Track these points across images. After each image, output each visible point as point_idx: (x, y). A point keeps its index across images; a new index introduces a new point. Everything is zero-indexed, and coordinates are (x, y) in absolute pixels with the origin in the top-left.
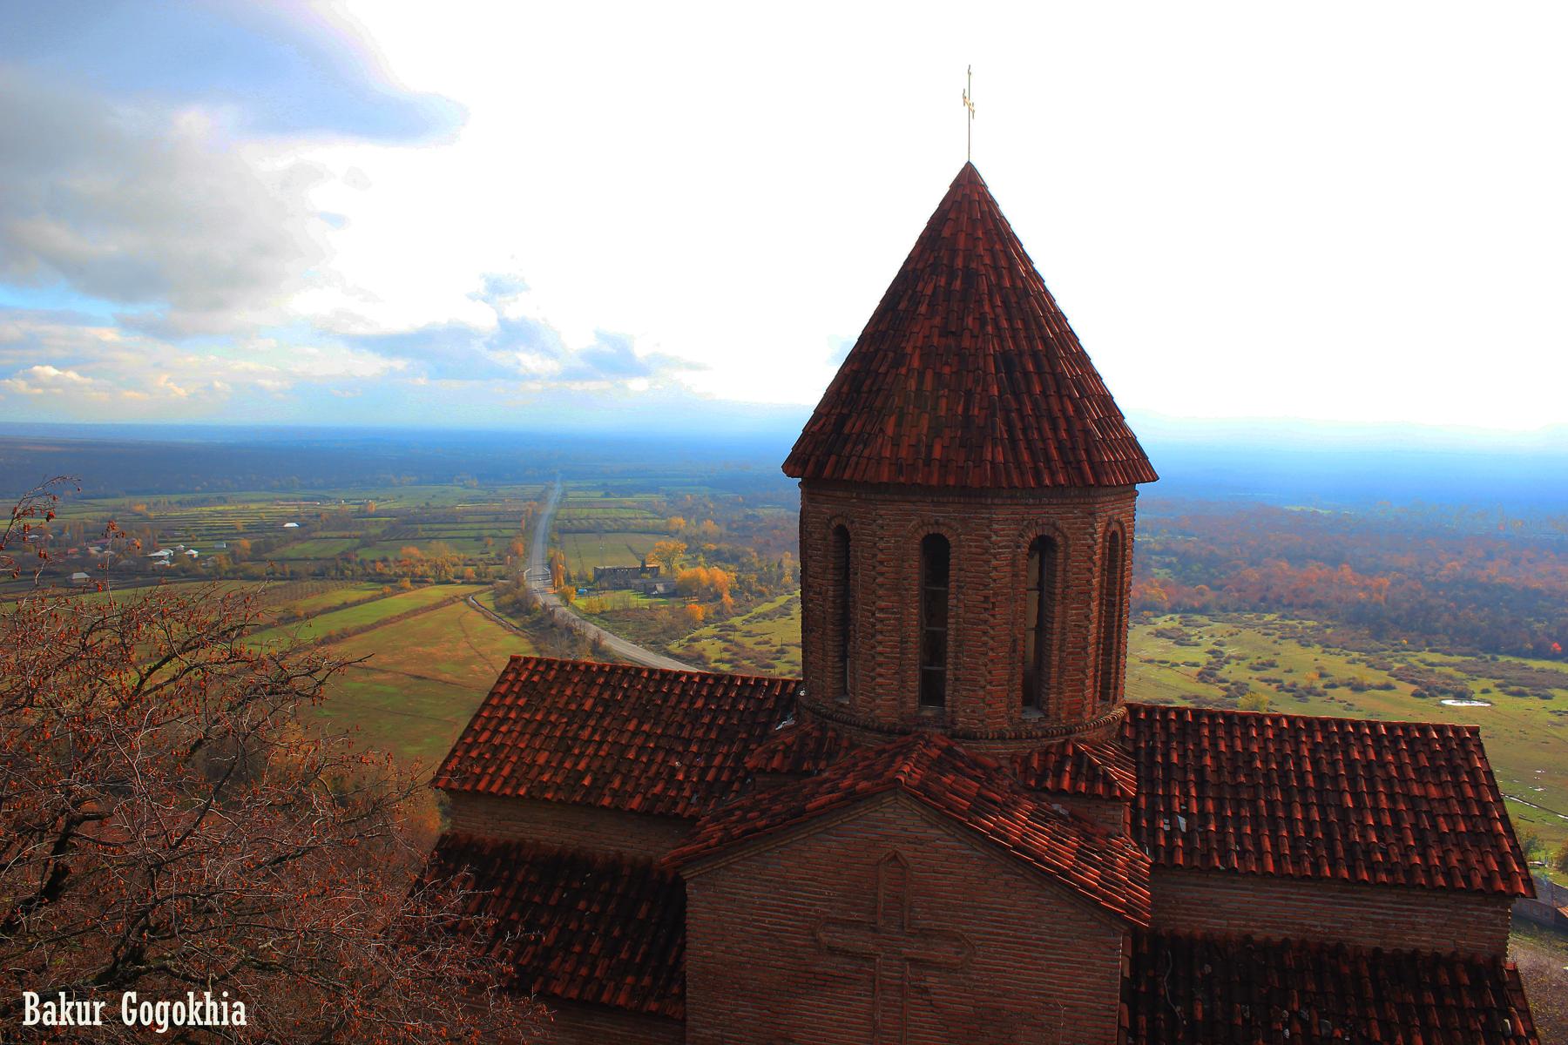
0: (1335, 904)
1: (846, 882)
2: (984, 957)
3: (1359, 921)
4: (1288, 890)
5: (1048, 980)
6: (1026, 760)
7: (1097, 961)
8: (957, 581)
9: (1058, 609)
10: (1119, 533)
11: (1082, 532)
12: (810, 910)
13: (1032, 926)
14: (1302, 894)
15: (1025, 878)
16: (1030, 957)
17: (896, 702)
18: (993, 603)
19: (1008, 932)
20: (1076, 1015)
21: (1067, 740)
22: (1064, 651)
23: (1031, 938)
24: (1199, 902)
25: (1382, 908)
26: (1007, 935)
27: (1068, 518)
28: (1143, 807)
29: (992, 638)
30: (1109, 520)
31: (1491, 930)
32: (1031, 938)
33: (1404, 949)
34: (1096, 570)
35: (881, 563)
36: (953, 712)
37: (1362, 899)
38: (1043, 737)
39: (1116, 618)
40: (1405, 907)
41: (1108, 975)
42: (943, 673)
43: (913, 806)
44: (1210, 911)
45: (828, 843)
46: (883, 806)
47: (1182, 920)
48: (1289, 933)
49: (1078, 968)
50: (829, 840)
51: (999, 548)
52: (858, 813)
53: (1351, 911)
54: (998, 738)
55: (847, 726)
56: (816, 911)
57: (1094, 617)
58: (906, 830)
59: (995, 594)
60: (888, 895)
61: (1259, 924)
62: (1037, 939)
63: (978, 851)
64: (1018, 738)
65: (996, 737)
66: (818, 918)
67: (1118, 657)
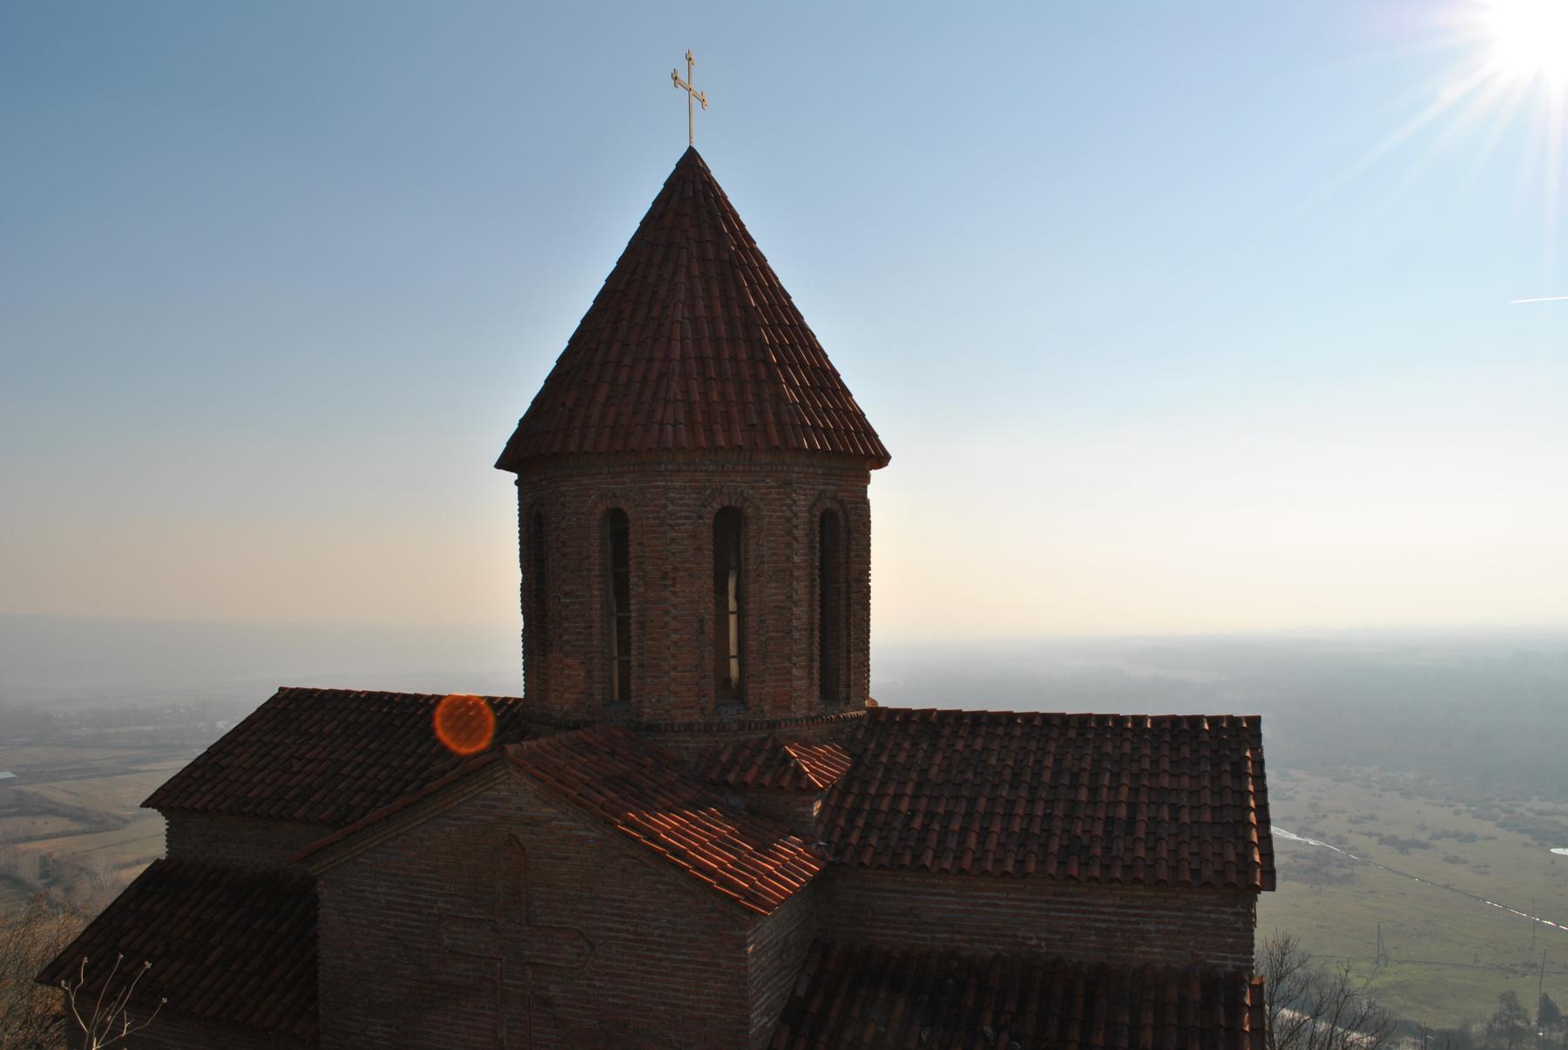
4: (996, 894)
10: (840, 513)
12: (432, 908)
13: (653, 920)
14: (1014, 899)
18: (674, 579)
19: (629, 927)
25: (1104, 913)
26: (628, 932)
30: (820, 495)
37: (1085, 904)
40: (1131, 911)
42: (630, 662)
46: (498, 781)
48: (1000, 947)
51: (680, 518)
56: (439, 908)
61: (966, 937)
62: (660, 936)
63: (592, 831)
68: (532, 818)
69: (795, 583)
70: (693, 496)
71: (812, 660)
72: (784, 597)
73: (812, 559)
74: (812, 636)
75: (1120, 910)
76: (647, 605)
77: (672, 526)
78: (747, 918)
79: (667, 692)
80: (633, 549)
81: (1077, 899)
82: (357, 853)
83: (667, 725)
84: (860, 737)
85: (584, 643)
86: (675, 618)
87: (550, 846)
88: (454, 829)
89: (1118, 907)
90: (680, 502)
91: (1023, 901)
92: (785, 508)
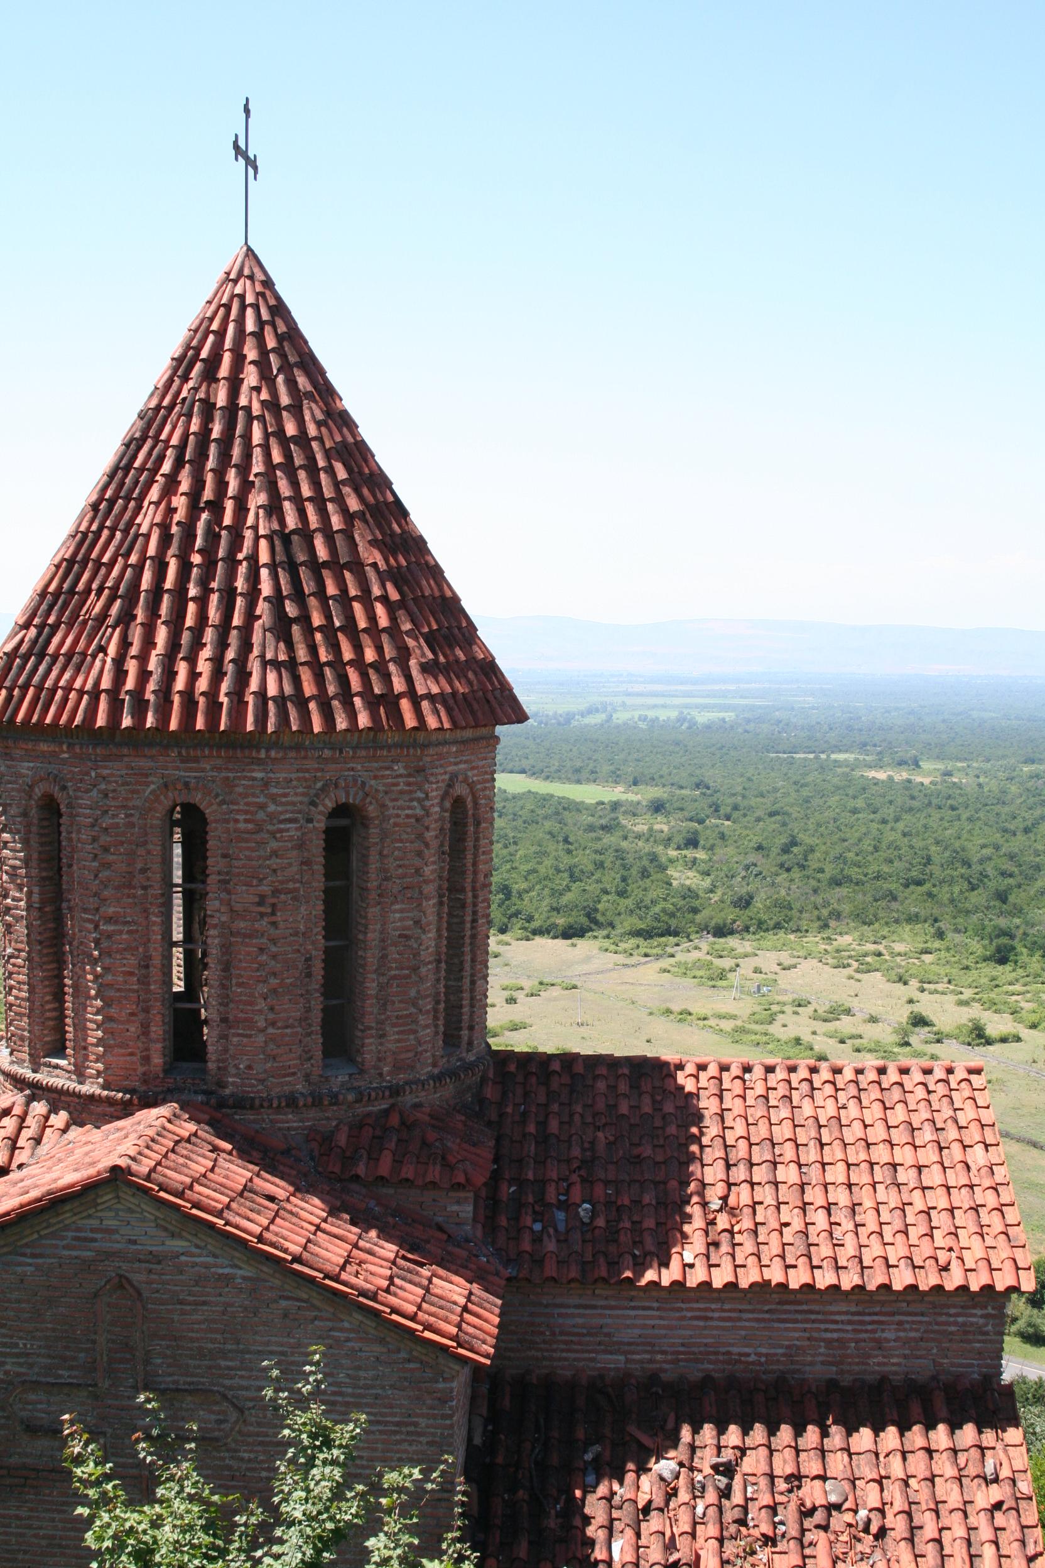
0: (773, 1321)
1: (49, 1326)
2: (259, 1424)
3: (807, 1343)
6: (327, 1139)
7: (420, 1420)
8: (219, 873)
9: (373, 911)
10: (469, 799)
11: (406, 797)
14: (730, 1311)
15: (313, 1306)
17: (134, 1058)
18: (274, 905)
21: (393, 1106)
22: (383, 975)
24: (585, 1331)
25: (836, 1322)
27: (383, 776)
28: (505, 1199)
29: (274, 957)
30: (451, 779)
31: (979, 1341)
33: (867, 1377)
34: (431, 855)
35: (106, 849)
36: (219, 1068)
37: (811, 1312)
38: (356, 1101)
39: (468, 925)
40: (867, 1318)
41: (437, 1439)
43: (143, 1206)
44: (600, 1344)
45: (19, 1269)
46: (99, 1208)
47: (560, 1359)
48: (711, 1367)
49: (395, 1433)
50: (20, 1264)
51: (281, 822)
52: (62, 1221)
53: (795, 1330)
54: (288, 1105)
55: (63, 1098)
57: (429, 924)
58: (135, 1242)
59: (276, 892)
61: (669, 1357)
63: (241, 1268)
64: (317, 1101)
65: (283, 1104)
66: (11, 1383)
67: (473, 982)
69: (424, 903)
70: (301, 790)
71: (438, 1002)
72: (411, 923)
73: (442, 868)
74: (438, 969)
75: (856, 1318)
76: (233, 939)
77: (273, 834)
78: (457, 1367)
79: (262, 1056)
80: (215, 863)
81: (805, 1307)
84: (489, 1096)
85: (135, 987)
86: (274, 957)
88: (32, 1269)
89: (853, 1314)
90: (284, 800)
91: (740, 1311)
92: (415, 803)
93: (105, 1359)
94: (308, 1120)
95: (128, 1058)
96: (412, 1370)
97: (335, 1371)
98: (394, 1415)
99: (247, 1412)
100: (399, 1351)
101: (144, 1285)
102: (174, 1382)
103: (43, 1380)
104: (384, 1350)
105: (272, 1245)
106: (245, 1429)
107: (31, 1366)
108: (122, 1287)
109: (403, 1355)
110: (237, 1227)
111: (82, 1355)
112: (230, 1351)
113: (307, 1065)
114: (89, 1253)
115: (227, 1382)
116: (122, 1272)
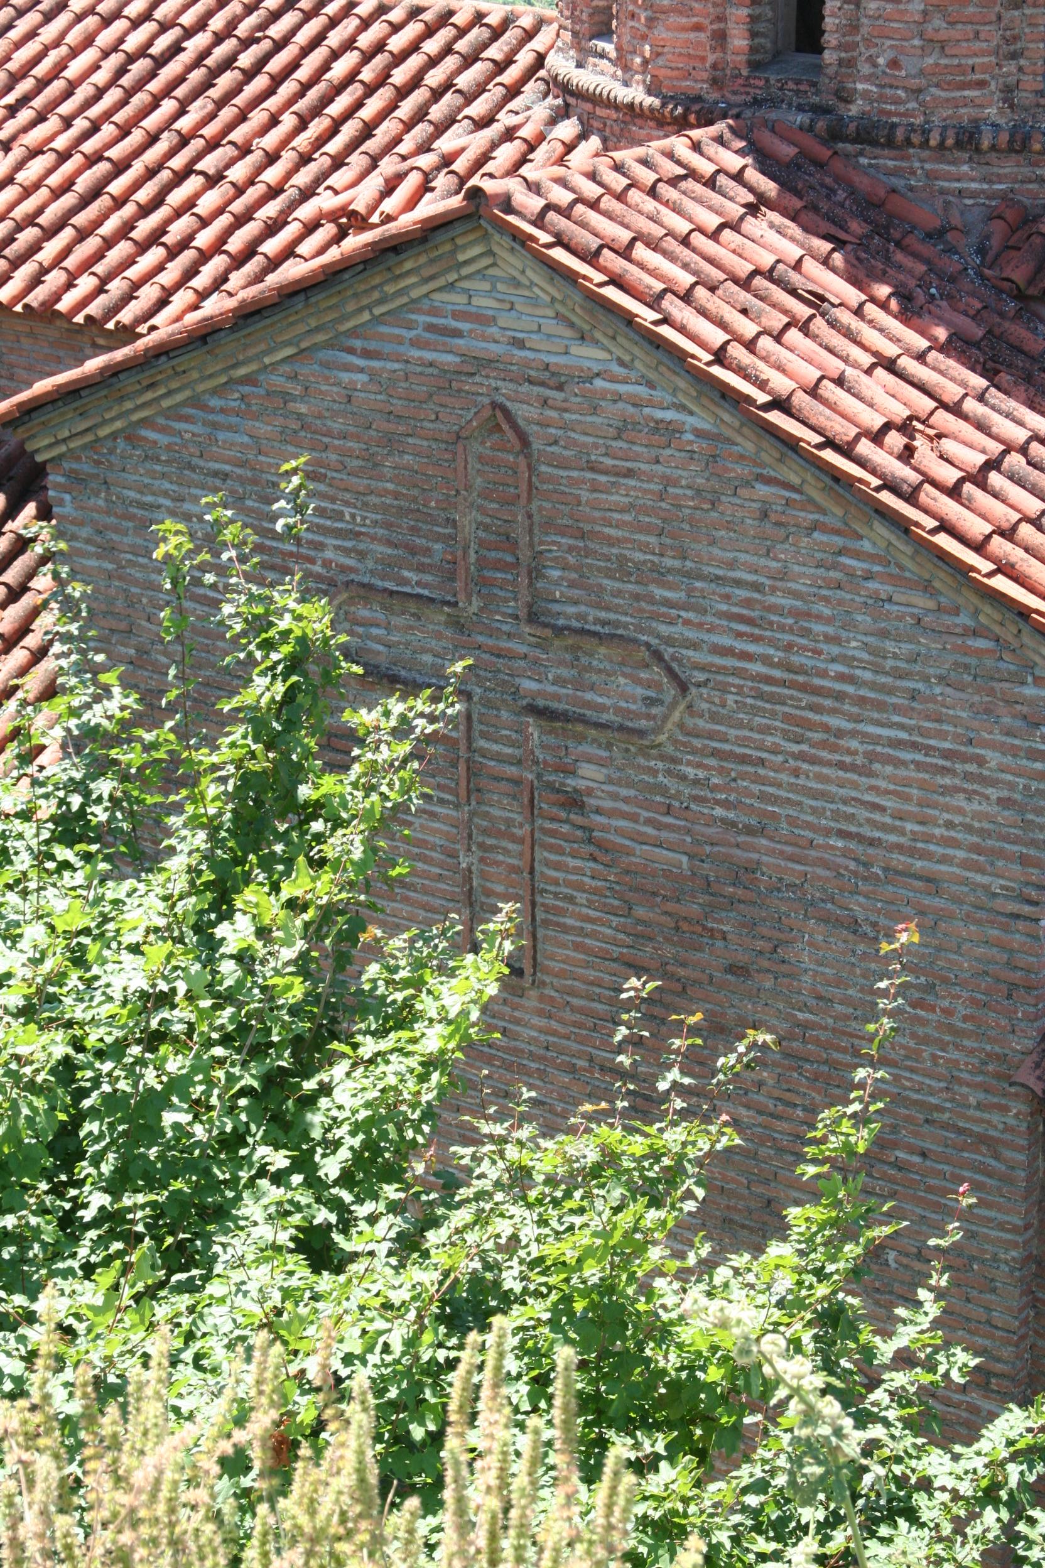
1: (390, 486)
2: (714, 718)
5: (868, 797)
13: (829, 639)
15: (811, 501)
16: (826, 728)
17: (702, 36)
19: (771, 651)
20: (938, 902)
23: (824, 674)
26: (766, 660)
32: (824, 674)
41: (1017, 797)
43: (529, 273)
45: (345, 377)
46: (465, 271)
49: (944, 771)
50: (348, 368)
54: (959, 145)
56: (326, 564)
58: (520, 344)
60: (486, 528)
62: (841, 678)
63: (691, 413)
65: (950, 142)
68: (547, 367)
79: (916, 42)
82: (135, 417)
83: (912, 128)
87: (590, 440)
88: (363, 378)
93: (473, 557)
94: (1000, 179)
95: (692, 35)
96: (979, 653)
97: (844, 634)
98: (942, 735)
99: (694, 690)
100: (956, 612)
101: (535, 428)
102: (580, 617)
103: (380, 583)
104: (931, 604)
105: (742, 371)
106: (690, 722)
107: (362, 555)
108: (498, 428)
109: (964, 619)
110: (682, 329)
111: (438, 547)
112: (670, 571)
113: (1010, 67)
114: (450, 358)
115: (664, 629)
116: (500, 399)
